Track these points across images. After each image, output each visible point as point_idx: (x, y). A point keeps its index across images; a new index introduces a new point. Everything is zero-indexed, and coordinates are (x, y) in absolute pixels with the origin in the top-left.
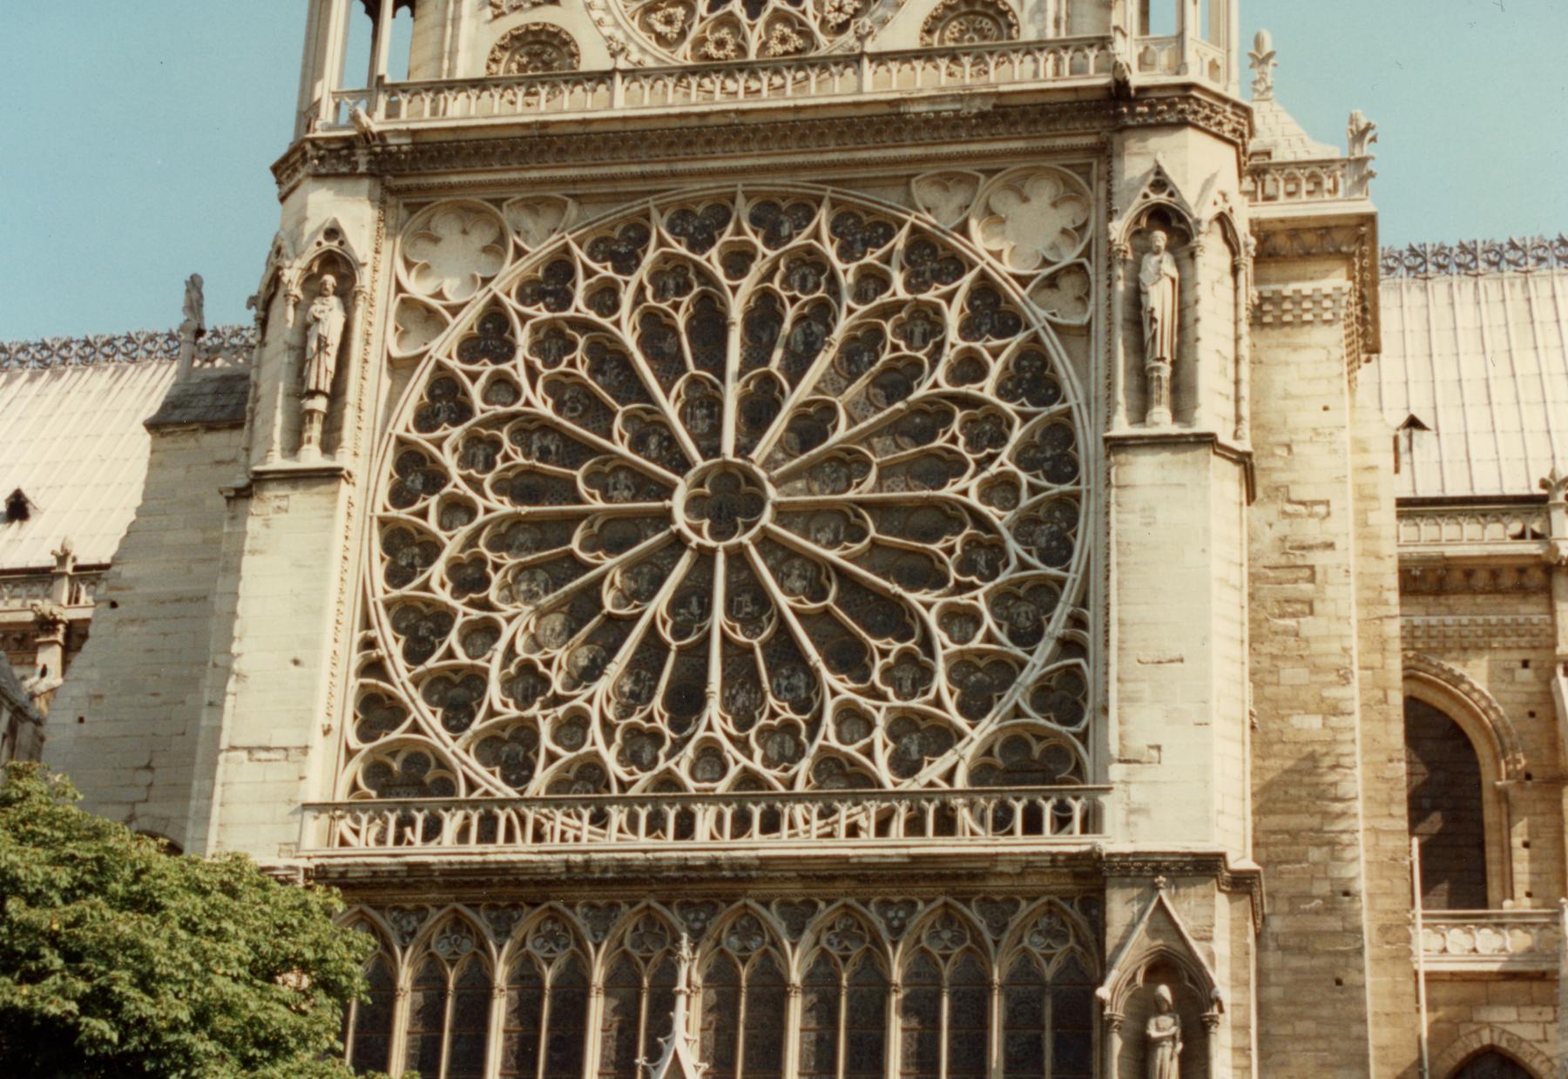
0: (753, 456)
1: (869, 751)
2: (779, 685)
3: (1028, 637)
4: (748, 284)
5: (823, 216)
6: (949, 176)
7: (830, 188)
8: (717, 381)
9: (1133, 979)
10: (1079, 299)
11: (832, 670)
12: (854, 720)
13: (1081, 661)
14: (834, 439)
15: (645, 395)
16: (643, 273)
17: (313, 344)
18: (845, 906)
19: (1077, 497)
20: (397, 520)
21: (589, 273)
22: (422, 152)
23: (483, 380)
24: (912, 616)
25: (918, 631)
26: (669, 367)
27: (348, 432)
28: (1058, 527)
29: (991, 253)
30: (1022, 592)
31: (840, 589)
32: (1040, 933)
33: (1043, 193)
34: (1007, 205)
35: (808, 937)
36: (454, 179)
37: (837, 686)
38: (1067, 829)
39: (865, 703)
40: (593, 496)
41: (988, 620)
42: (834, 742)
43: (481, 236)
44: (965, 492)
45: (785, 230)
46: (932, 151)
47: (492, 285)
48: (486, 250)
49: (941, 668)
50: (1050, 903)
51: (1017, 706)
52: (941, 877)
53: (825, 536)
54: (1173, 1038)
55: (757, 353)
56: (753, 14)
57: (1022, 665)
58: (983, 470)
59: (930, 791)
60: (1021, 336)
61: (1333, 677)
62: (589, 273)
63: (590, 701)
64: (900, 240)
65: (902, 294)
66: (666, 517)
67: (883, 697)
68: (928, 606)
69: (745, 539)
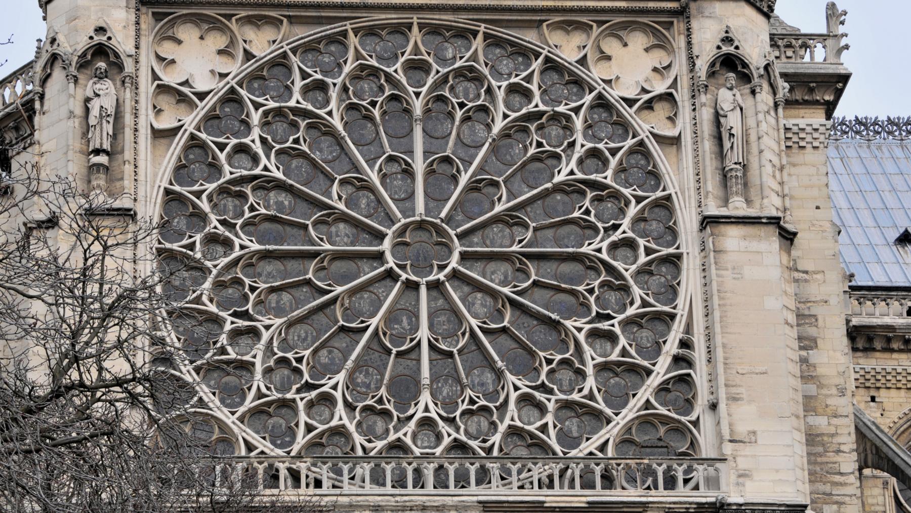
2: (472, 381)
6: (570, 23)
7: (483, 25)
10: (669, 118)
13: (691, 371)
17: (95, 112)
19: (679, 257)
26: (368, 145)
29: (603, 81)
31: (512, 315)
33: (638, 41)
34: (611, 46)
37: (516, 384)
38: (692, 484)
39: (540, 396)
43: (218, 41)
44: (599, 250)
48: (220, 52)
51: (648, 401)
53: (499, 276)
57: (649, 372)
58: (609, 236)
61: (834, 391)
62: (304, 75)
63: (335, 387)
65: (542, 107)
66: (379, 257)
67: (551, 392)
68: (579, 330)
69: (441, 276)
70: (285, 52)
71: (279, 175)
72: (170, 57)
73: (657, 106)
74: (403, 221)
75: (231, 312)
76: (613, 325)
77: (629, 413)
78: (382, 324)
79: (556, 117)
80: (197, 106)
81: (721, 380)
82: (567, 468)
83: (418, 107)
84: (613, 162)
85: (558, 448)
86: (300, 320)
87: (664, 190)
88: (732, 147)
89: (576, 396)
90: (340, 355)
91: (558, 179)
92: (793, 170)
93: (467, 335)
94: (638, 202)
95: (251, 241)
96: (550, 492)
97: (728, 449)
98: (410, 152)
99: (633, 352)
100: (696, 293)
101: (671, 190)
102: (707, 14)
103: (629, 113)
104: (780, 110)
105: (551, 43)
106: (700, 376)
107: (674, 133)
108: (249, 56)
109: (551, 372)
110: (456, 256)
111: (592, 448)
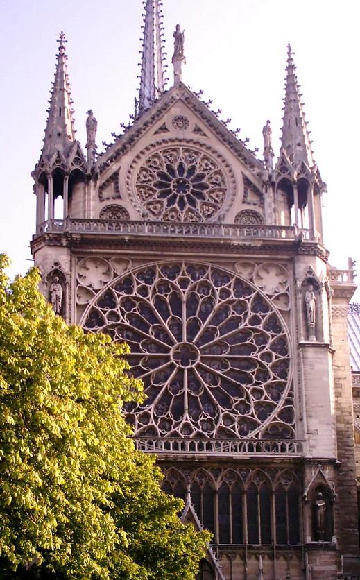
0: (194, 341)
1: (233, 428)
3: (278, 398)
5: (209, 272)
6: (246, 264)
15: (158, 321)
19: (288, 360)
21: (138, 283)
22: (84, 241)
30: (274, 386)
33: (273, 272)
34: (263, 274)
35: (220, 478)
36: (94, 250)
37: (222, 411)
41: (266, 393)
43: (102, 269)
45: (197, 275)
46: (242, 255)
48: (104, 273)
51: (275, 417)
52: (257, 463)
53: (216, 367)
56: (182, 209)
57: (276, 406)
62: (138, 283)
63: (150, 410)
64: (232, 281)
65: (234, 298)
66: (168, 358)
67: (236, 413)
69: (193, 366)
71: (128, 324)
72: (84, 275)
73: (281, 298)
79: (240, 302)
82: (242, 443)
83: (184, 297)
84: (263, 321)
85: (239, 436)
89: (246, 415)
92: (334, 325)
96: (236, 453)
97: (306, 436)
98: (181, 316)
102: (302, 261)
103: (269, 301)
105: (238, 271)
107: (288, 309)
108: (115, 275)
110: (199, 358)
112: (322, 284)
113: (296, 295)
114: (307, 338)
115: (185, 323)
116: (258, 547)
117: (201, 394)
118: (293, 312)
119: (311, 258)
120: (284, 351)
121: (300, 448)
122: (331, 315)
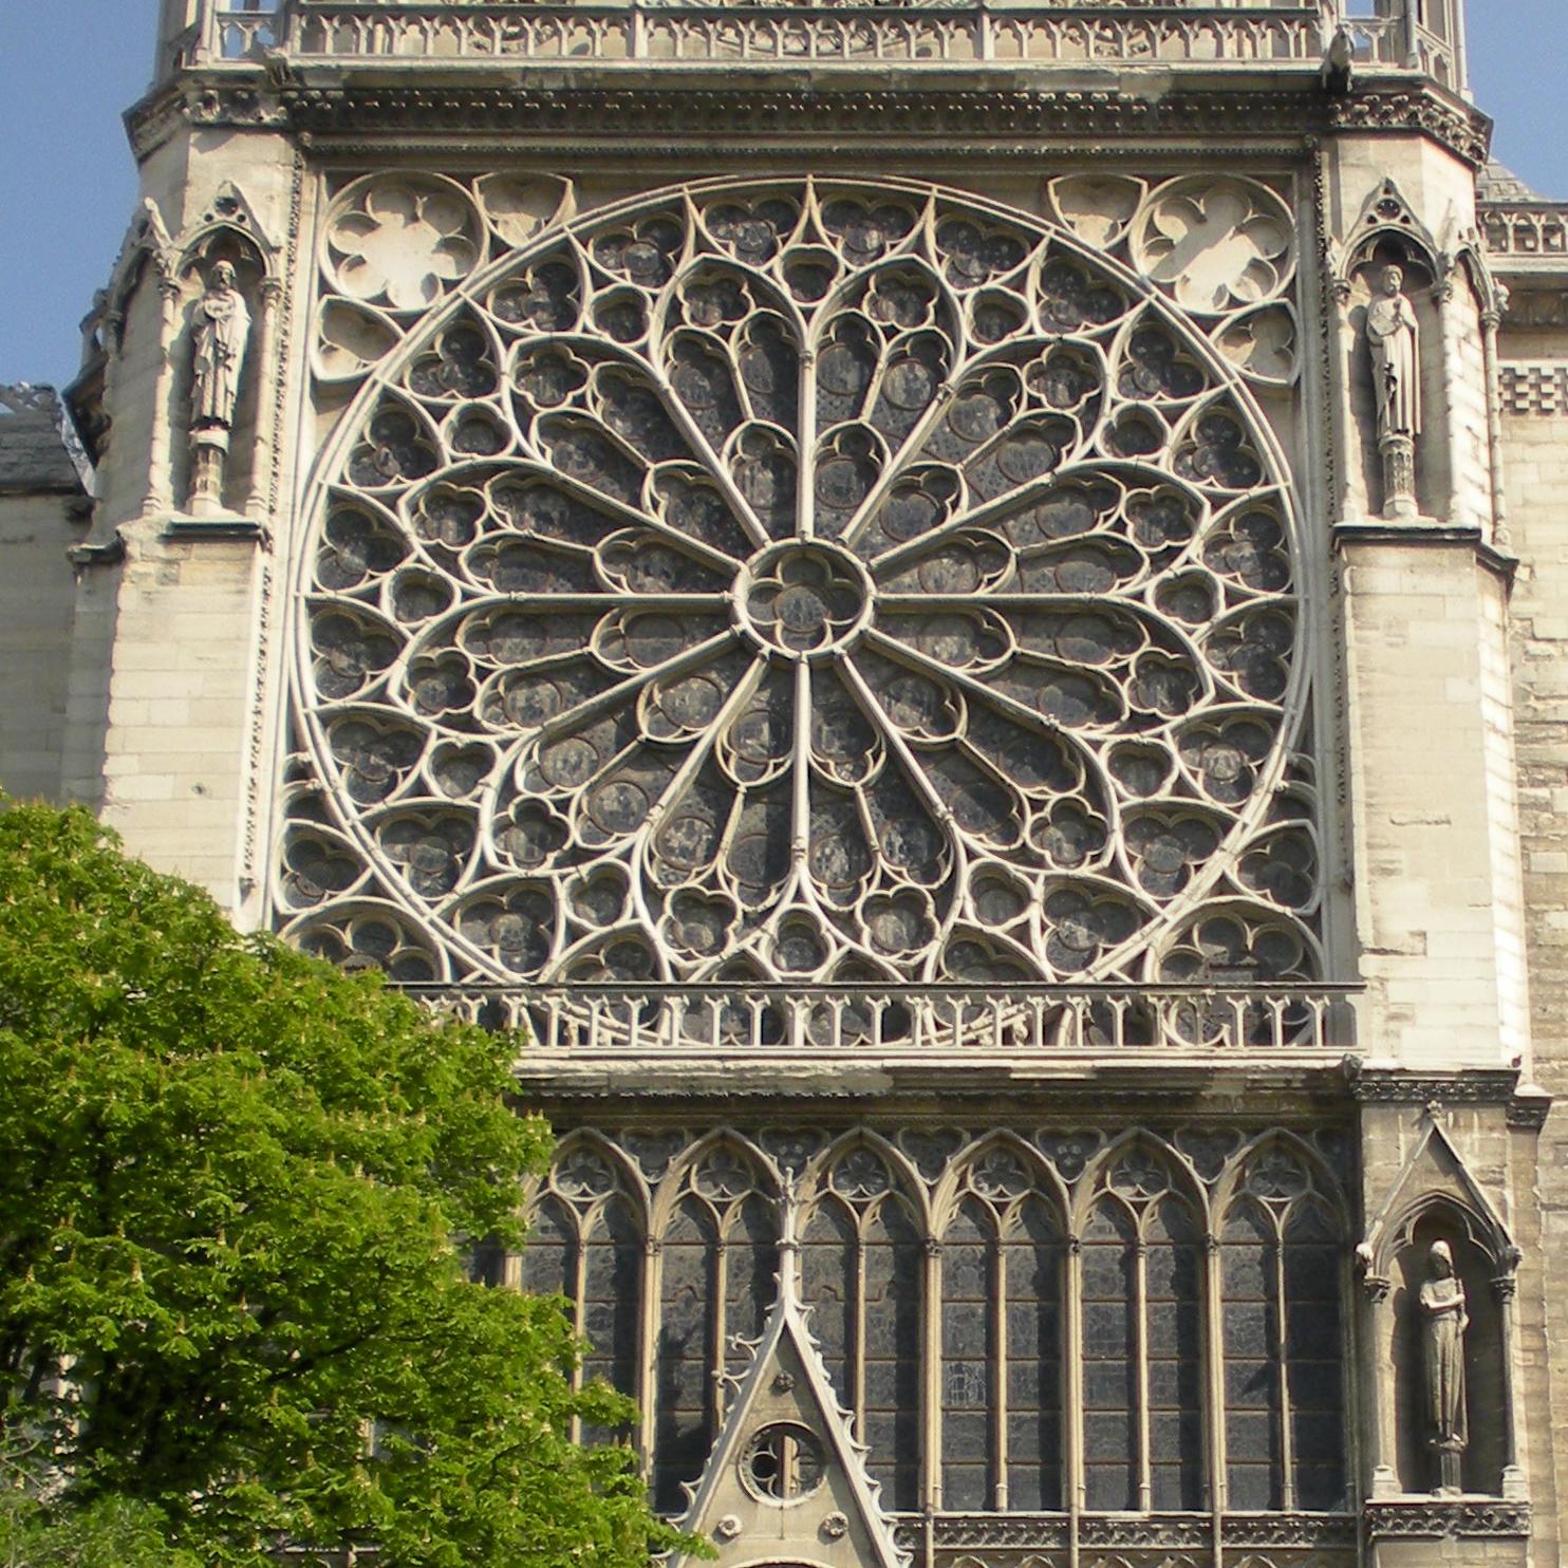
0: (846, 535)
1: (1022, 932)
2: (890, 844)
4: (825, 308)
5: (928, 223)
7: (935, 187)
8: (789, 435)
9: (1401, 1234)
10: (1279, 352)
11: (964, 826)
12: (1000, 891)
14: (952, 520)
16: (676, 286)
17: (207, 352)
18: (1001, 1137)
19: (1289, 608)
20: (335, 603)
21: (600, 281)
23: (452, 416)
24: (1072, 757)
25: (1083, 777)
27: (261, 479)
28: (1265, 645)
32: (1264, 1176)
35: (950, 1179)
36: (402, 143)
37: (975, 845)
38: (1303, 1035)
40: (617, 582)
42: (973, 921)
47: (460, 289)
49: (1117, 823)
50: (1279, 1137)
51: (1223, 878)
52: (1133, 1101)
54: (1456, 1307)
55: (842, 398)
57: (1226, 825)
58: (1160, 570)
59: (1110, 985)
60: (1206, 396)
62: (600, 281)
63: (627, 856)
64: (1036, 259)
65: (1041, 333)
66: (723, 615)
67: (1039, 862)
68: (1096, 745)
69: (838, 648)
70: (567, 240)
71: (546, 463)
72: (354, 252)
74: (770, 545)
75: (439, 716)
76: (1161, 736)
77: (1185, 903)
78: (723, 737)
80: (397, 339)
81: (1360, 836)
82: (1061, 1010)
85: (1048, 970)
86: (571, 731)
87: (1267, 483)
88: (1393, 402)
90: (641, 796)
91: (1067, 464)
93: (883, 756)
94: (1215, 508)
95: (486, 585)
99: (1198, 785)
100: (1320, 676)
101: (1281, 485)
102: (1351, 160)
104: (1492, 336)
106: (1322, 836)
108: (499, 248)
109: (1039, 827)
110: (868, 612)
111: (1113, 968)
112: (1443, 257)
113: (1324, 311)
114: (1378, 501)
115: (810, 444)
116: (1129, 1528)
117: (874, 771)
118: (1314, 389)
119: (1399, 144)
120: (1274, 570)
121: (1340, 1027)
122: (1497, 404)
